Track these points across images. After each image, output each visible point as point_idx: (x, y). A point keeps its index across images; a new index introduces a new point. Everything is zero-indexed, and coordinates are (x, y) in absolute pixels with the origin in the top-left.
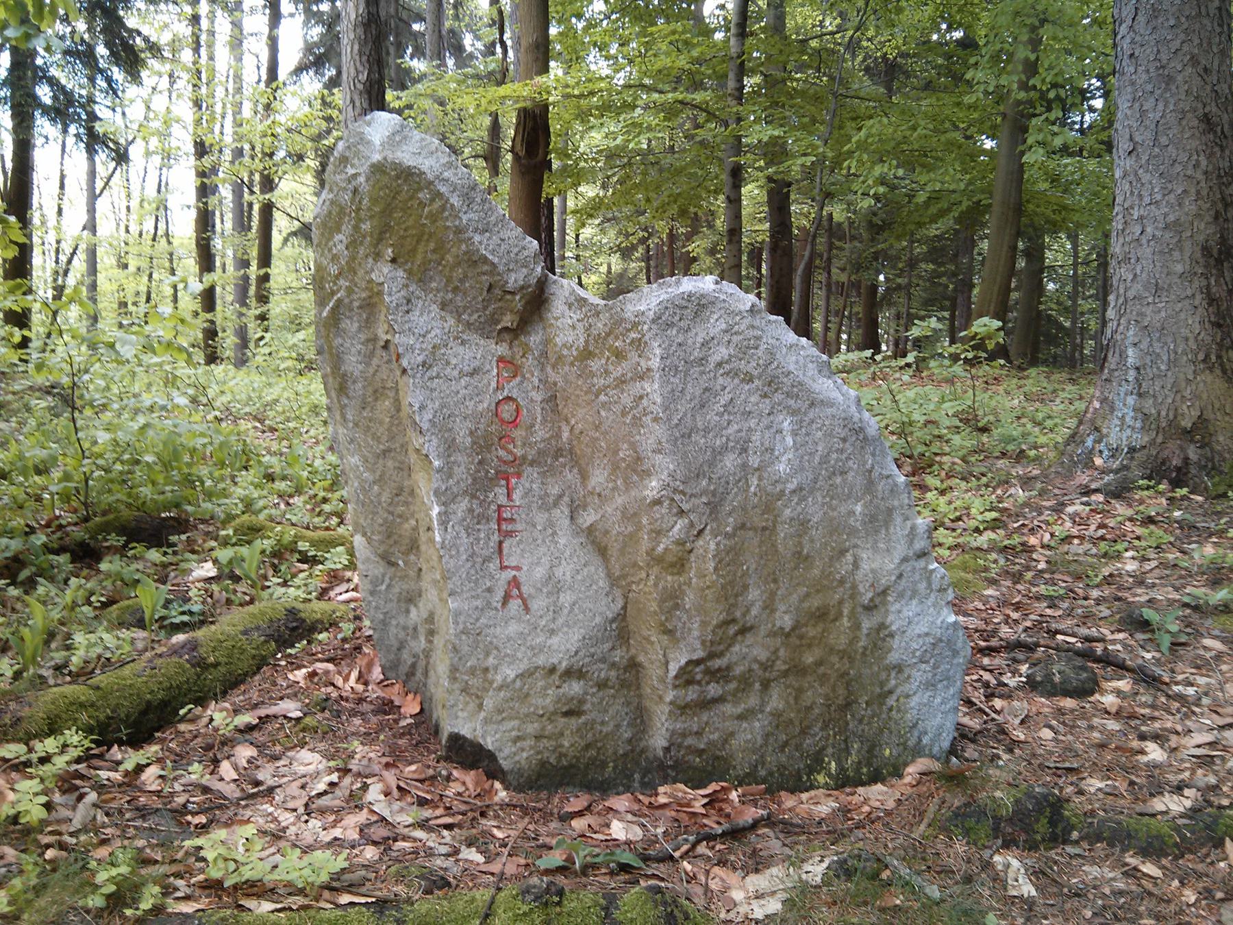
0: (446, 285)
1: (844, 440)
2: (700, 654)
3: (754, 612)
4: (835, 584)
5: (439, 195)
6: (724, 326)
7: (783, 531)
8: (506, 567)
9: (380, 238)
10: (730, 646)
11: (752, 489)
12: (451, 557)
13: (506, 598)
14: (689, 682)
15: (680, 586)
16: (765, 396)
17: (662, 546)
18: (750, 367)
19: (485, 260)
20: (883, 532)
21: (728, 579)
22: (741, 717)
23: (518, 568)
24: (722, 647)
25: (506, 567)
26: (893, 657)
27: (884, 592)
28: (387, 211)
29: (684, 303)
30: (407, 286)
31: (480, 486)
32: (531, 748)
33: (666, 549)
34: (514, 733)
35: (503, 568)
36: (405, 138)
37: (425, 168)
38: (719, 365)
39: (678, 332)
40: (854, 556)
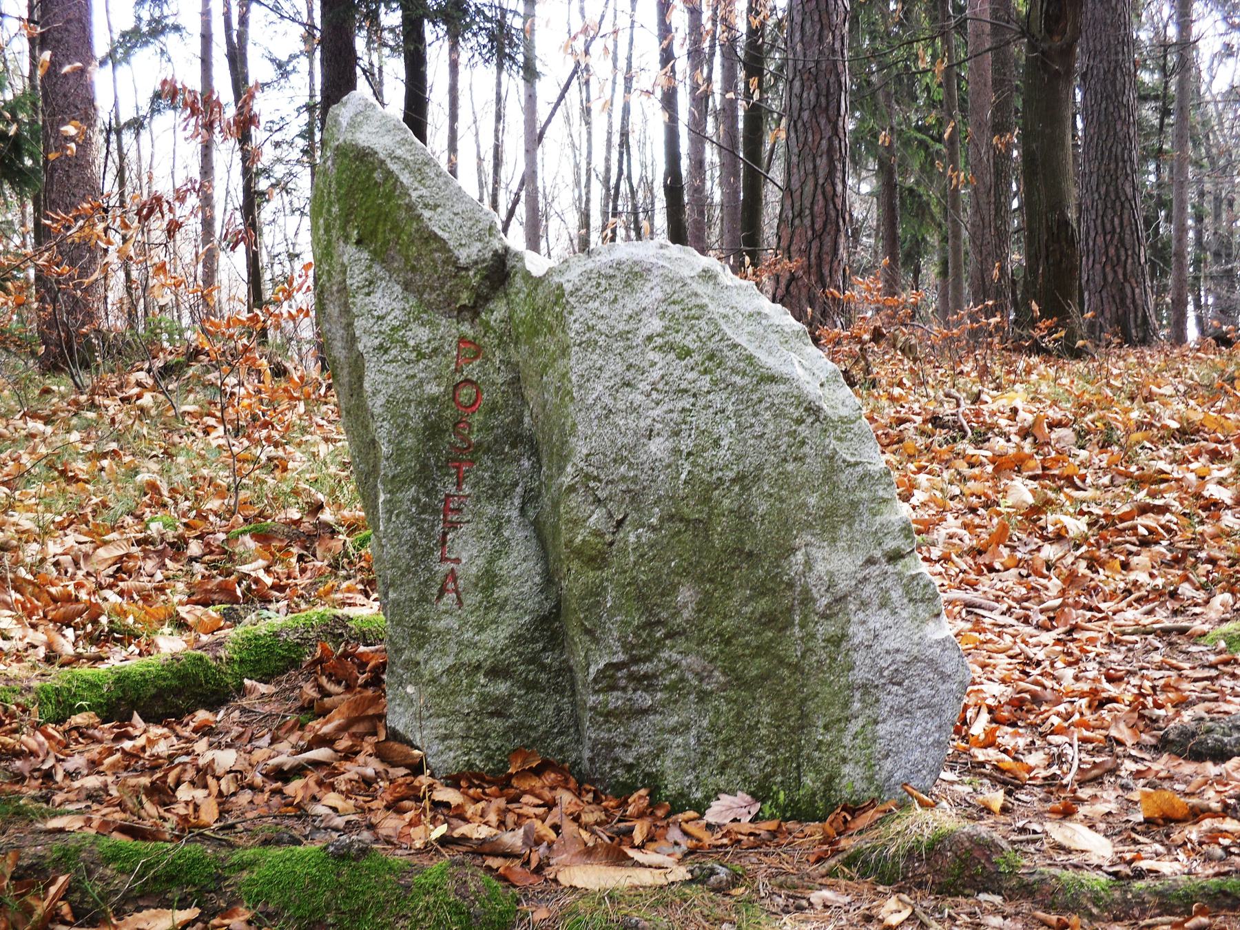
0: (406, 265)
1: (800, 421)
2: (621, 657)
3: (686, 614)
4: (783, 586)
5: (389, 173)
6: (660, 295)
7: (722, 524)
8: (447, 559)
9: (346, 218)
10: (657, 650)
11: (683, 477)
12: (393, 546)
13: (442, 591)
14: (612, 688)
15: (602, 582)
16: (706, 372)
17: (580, 538)
18: (690, 342)
19: (436, 237)
20: (845, 528)
21: (651, 576)
22: (674, 730)
23: (457, 561)
24: (645, 652)
25: (447, 559)
26: (860, 675)
27: (841, 599)
28: (350, 194)
29: (611, 272)
30: (370, 267)
31: (424, 476)
32: (459, 748)
33: (583, 541)
34: (442, 731)
35: (443, 559)
36: (367, 118)
37: (378, 148)
38: (650, 338)
39: (602, 304)
40: (807, 554)
